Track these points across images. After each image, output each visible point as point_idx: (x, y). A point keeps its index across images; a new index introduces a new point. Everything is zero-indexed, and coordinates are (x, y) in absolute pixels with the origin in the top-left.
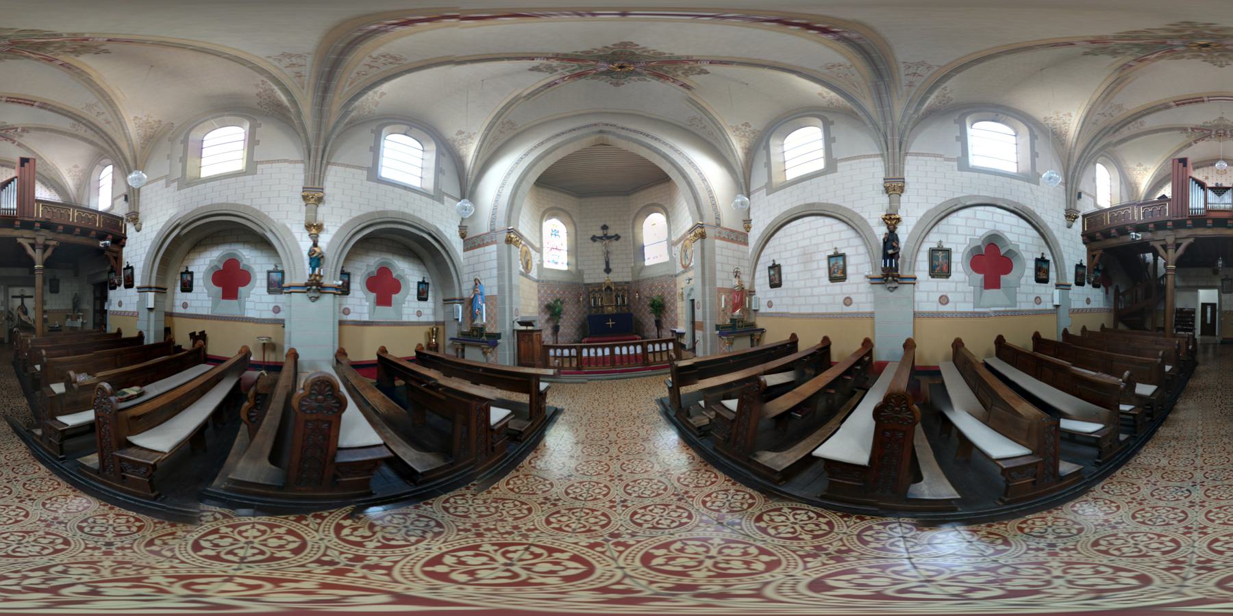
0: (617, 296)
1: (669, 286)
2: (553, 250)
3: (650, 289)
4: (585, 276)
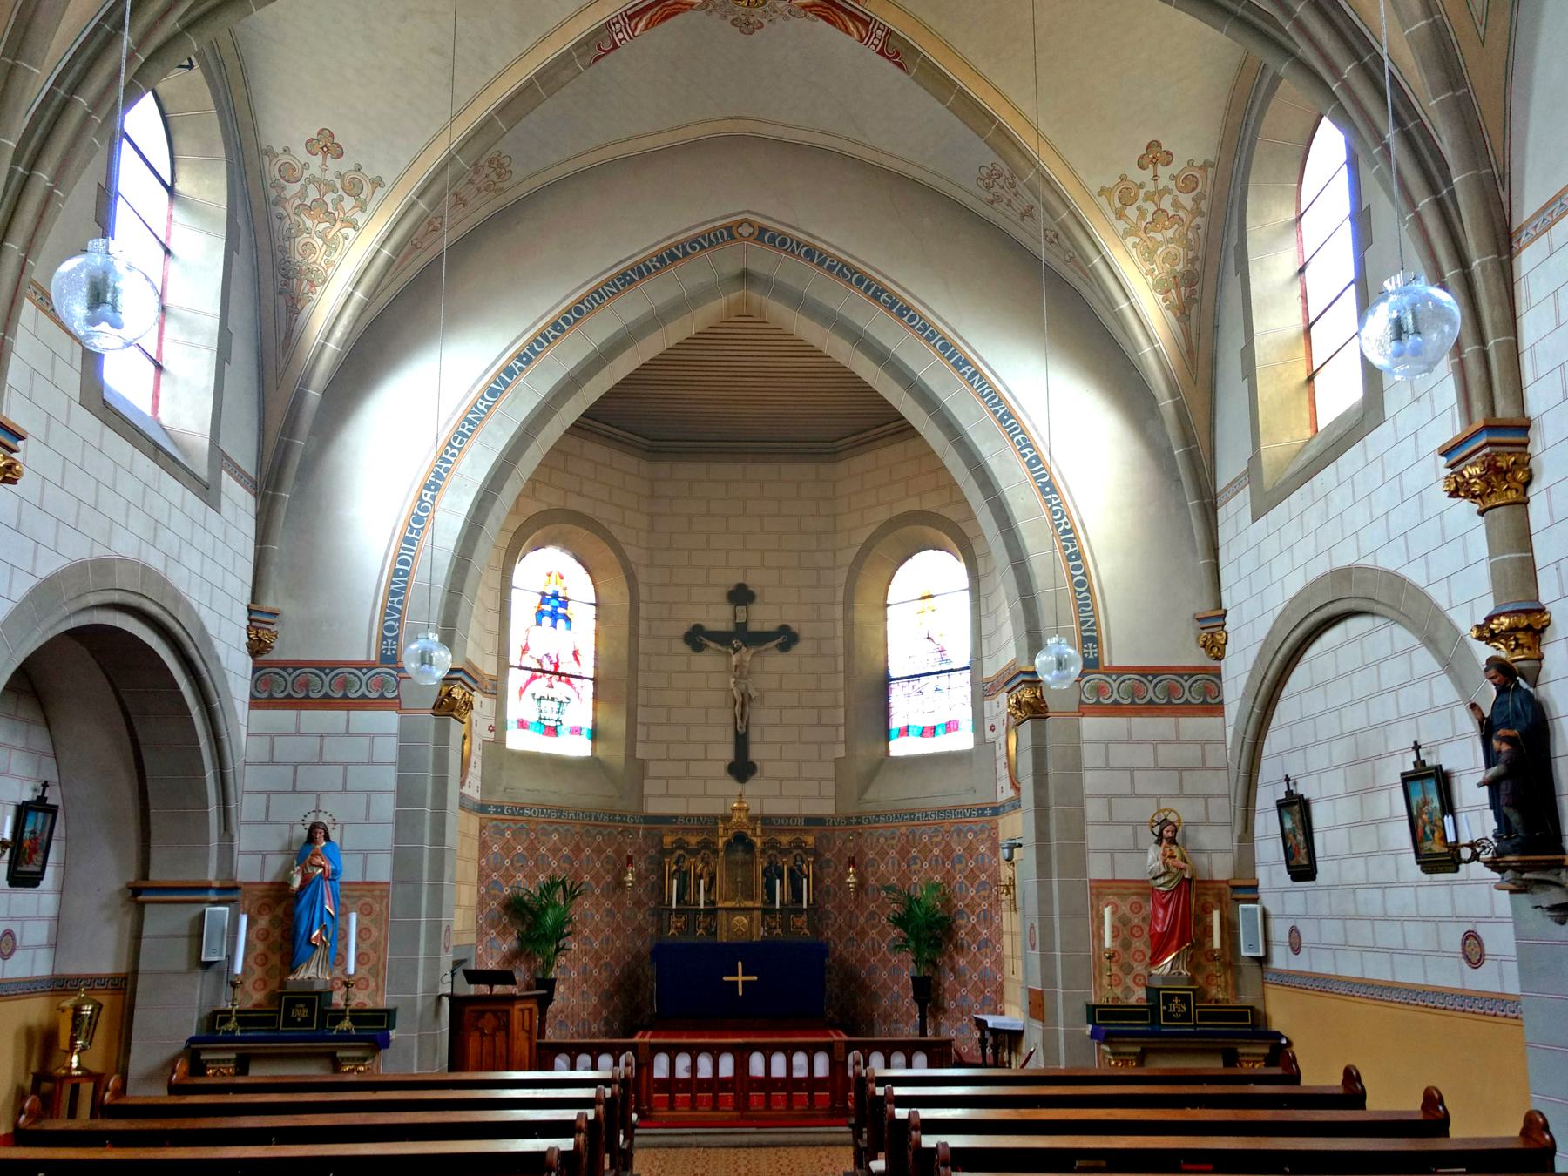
0: (772, 873)
1: (970, 849)
2: (543, 681)
3: (904, 853)
4: (649, 787)
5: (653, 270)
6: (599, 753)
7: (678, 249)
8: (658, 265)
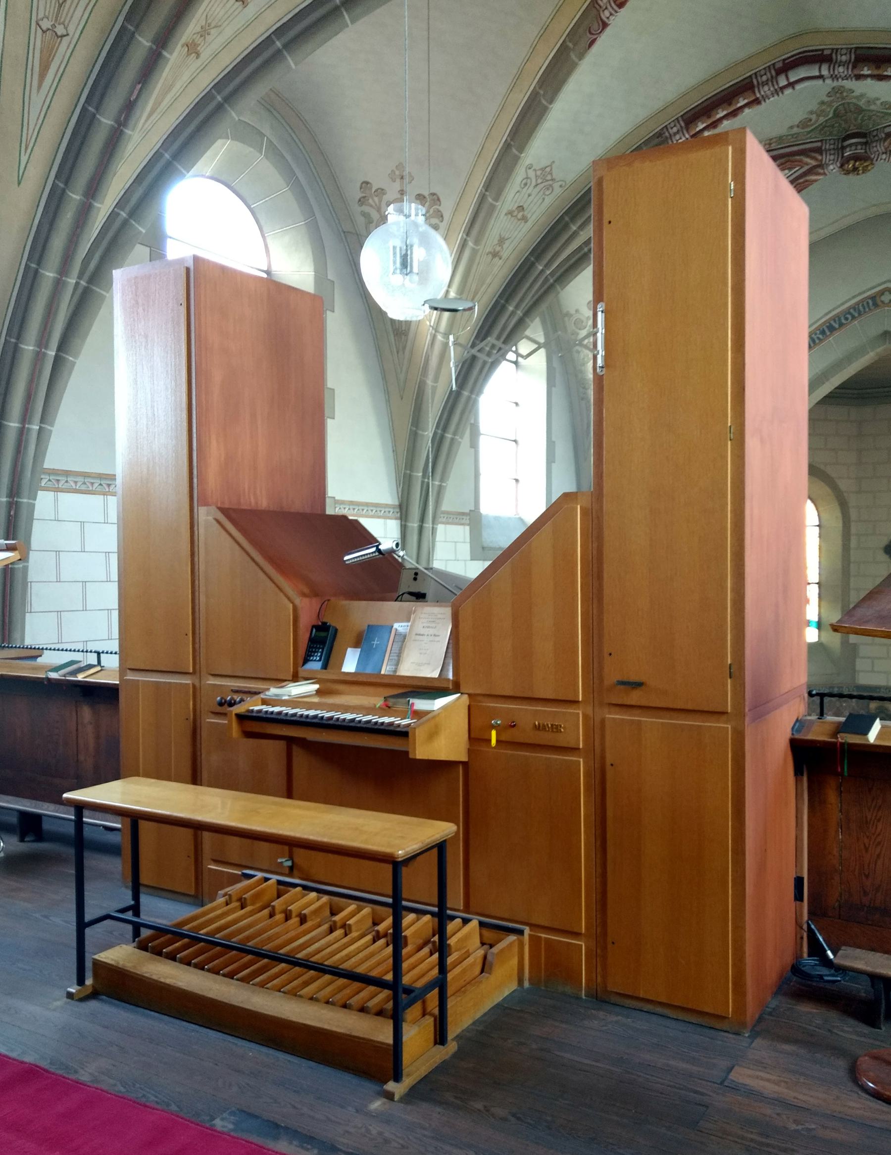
4: (860, 664)
5: (817, 341)
6: (823, 640)
7: (835, 321)
8: (821, 336)
